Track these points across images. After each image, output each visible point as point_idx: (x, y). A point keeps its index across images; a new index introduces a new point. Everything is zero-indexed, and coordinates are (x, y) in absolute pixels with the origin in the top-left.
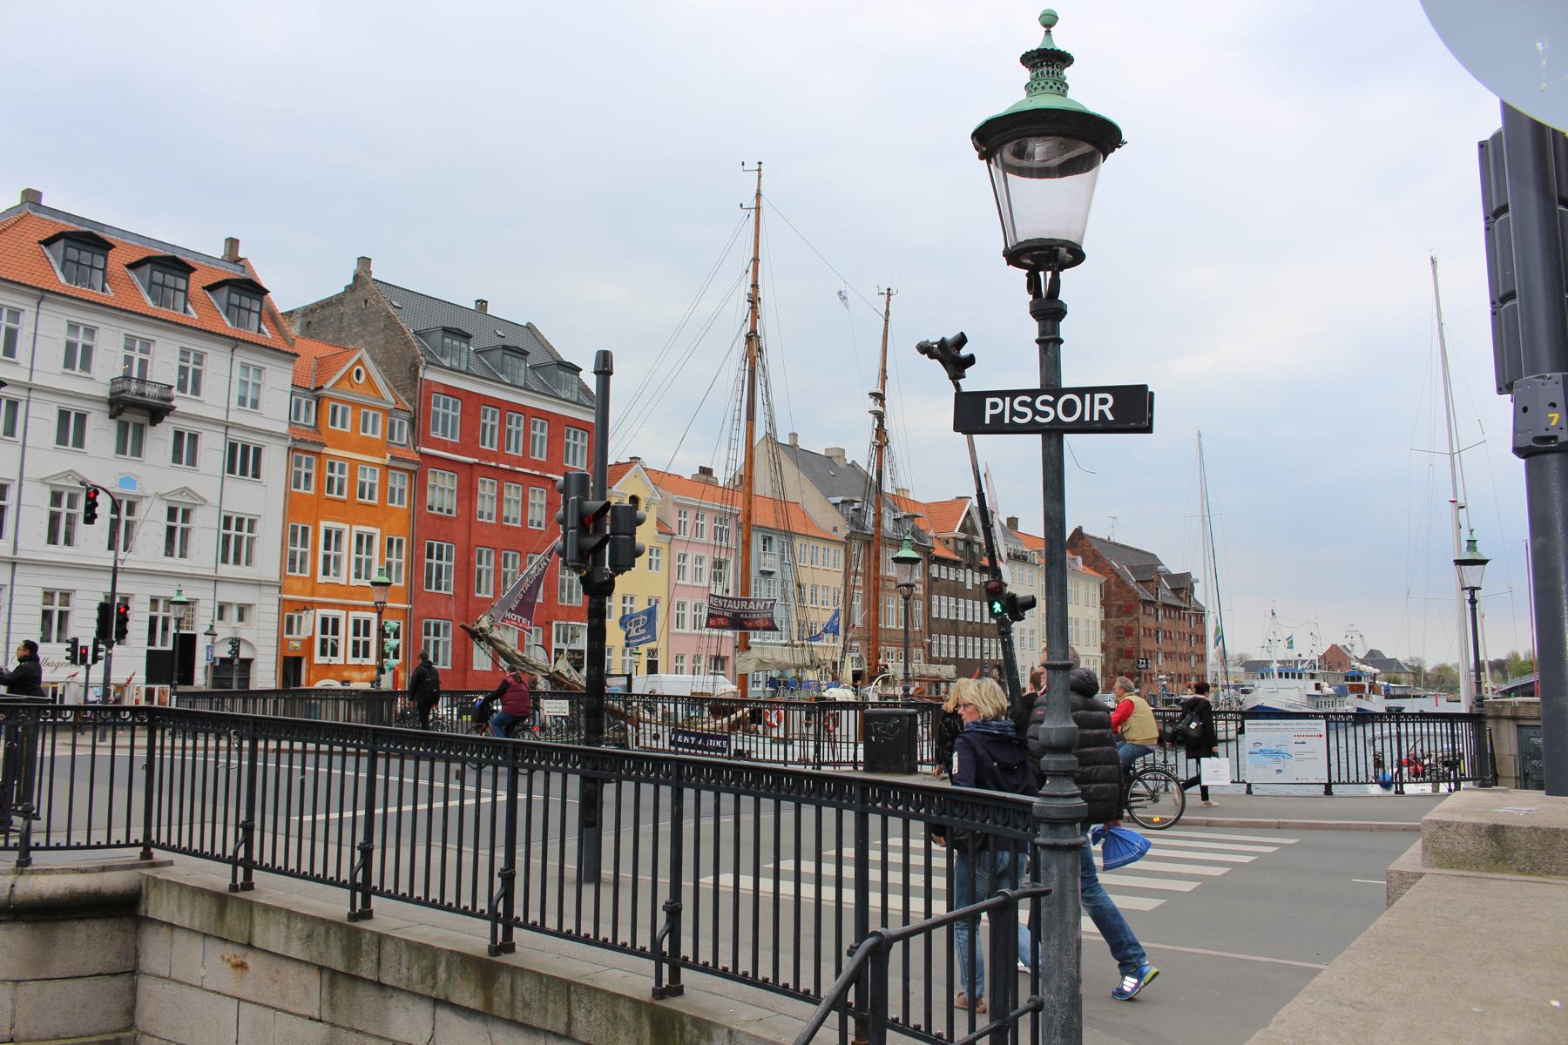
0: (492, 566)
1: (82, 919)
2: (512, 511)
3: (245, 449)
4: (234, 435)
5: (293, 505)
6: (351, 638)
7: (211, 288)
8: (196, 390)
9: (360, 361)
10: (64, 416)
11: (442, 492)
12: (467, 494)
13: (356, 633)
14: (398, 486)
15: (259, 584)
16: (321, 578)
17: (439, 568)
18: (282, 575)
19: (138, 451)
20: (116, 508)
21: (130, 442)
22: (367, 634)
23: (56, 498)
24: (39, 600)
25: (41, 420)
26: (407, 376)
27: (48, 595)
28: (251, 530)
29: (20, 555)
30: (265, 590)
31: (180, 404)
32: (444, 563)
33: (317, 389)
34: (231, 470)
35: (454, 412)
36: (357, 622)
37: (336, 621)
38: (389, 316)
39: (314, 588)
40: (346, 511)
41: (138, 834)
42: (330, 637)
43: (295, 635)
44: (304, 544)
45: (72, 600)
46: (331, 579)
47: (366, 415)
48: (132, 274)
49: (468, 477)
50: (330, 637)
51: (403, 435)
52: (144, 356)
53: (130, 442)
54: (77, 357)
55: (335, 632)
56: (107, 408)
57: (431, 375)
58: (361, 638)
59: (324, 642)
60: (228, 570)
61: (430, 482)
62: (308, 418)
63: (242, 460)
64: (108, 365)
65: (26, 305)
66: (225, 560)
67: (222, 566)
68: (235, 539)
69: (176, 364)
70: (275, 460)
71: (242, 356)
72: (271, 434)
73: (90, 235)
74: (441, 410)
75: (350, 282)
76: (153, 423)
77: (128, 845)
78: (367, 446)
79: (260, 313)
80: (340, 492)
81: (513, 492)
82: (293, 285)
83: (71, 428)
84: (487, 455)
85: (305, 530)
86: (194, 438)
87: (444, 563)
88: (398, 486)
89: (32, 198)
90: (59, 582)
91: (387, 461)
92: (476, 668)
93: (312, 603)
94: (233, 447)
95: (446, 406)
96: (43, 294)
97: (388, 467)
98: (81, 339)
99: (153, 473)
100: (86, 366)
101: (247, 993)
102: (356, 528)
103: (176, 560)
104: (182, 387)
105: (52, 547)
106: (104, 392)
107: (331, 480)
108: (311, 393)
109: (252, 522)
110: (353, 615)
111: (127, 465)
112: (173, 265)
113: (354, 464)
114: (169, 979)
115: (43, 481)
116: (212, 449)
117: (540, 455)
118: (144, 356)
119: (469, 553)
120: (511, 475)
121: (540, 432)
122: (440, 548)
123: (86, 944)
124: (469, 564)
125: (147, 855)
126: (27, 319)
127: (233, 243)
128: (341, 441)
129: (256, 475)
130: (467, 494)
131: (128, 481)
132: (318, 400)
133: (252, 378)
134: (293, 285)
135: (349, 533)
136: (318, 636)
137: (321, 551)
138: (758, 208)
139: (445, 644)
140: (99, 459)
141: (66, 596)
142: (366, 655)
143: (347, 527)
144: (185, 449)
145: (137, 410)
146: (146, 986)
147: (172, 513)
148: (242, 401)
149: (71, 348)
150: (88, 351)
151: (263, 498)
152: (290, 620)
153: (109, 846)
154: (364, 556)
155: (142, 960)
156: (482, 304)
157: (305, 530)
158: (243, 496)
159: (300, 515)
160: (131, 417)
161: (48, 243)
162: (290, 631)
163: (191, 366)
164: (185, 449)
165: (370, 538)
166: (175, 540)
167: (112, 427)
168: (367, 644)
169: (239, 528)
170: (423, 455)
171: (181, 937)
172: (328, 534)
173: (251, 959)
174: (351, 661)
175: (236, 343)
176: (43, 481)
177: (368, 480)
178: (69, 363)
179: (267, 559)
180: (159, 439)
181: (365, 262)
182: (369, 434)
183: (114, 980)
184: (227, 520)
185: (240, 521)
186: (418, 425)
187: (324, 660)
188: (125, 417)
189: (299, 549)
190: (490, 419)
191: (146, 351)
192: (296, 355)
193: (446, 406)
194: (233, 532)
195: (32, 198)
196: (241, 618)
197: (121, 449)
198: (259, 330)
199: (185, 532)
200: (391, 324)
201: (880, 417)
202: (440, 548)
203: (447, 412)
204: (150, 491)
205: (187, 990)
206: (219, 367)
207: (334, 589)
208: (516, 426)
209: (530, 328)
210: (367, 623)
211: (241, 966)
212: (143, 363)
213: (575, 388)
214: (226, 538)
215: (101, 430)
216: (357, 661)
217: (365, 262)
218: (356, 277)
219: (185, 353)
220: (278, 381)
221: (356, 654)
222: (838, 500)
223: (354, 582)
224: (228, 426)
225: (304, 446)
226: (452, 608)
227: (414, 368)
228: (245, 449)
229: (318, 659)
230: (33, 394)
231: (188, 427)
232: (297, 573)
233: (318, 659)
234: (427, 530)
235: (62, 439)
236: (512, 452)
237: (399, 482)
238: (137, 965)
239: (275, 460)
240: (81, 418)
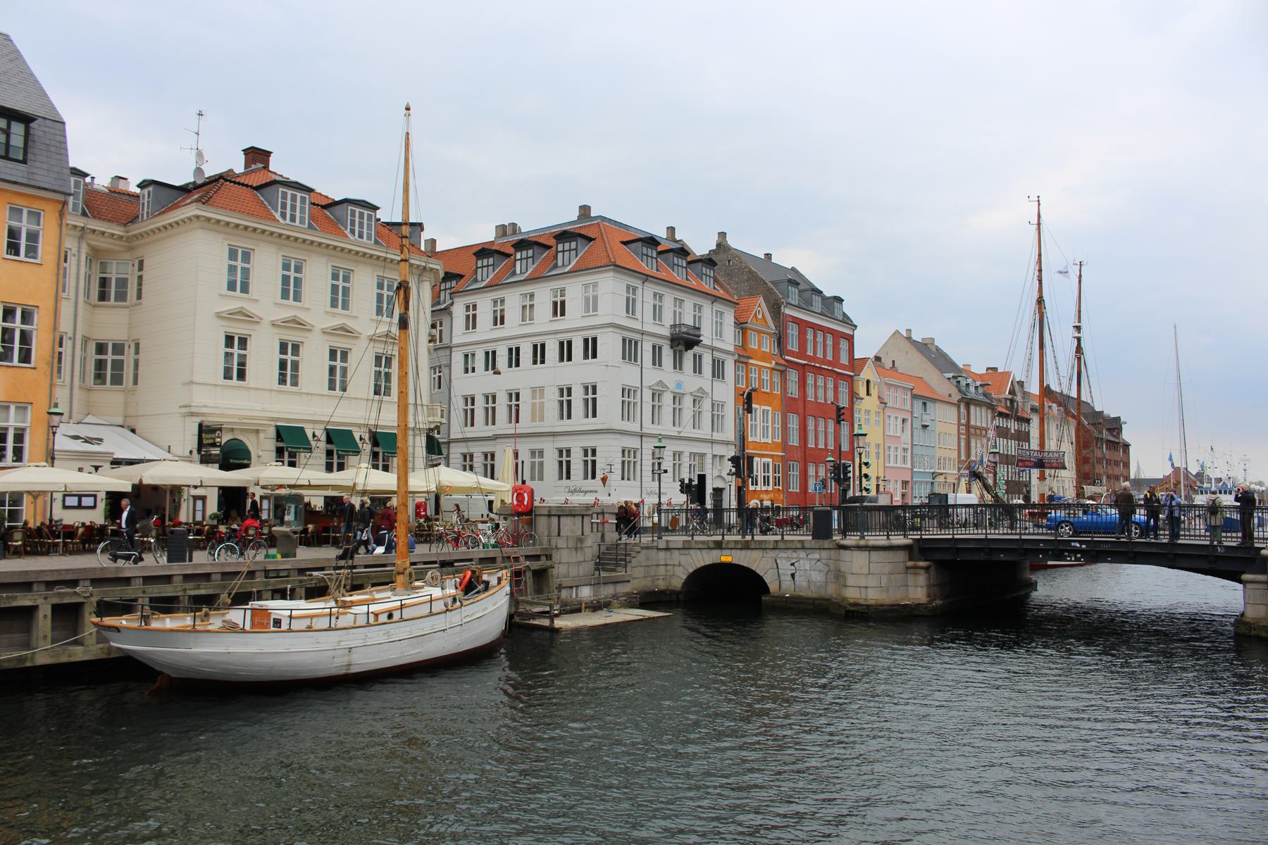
10: (654, 347)
12: (803, 384)
21: (678, 364)
26: (775, 309)
29: (644, 431)
53: (678, 364)
54: (657, 313)
57: (788, 311)
72: (728, 352)
111: (678, 376)
115: (650, 387)
117: (830, 357)
126: (639, 292)
130: (803, 384)
138: (1039, 224)
156: (768, 256)
167: (671, 352)
176: (650, 387)
180: (688, 357)
201: (1079, 339)
203: (793, 331)
204: (687, 391)
209: (793, 269)
218: (718, 245)
222: (950, 375)
224: (713, 349)
240: (660, 348)
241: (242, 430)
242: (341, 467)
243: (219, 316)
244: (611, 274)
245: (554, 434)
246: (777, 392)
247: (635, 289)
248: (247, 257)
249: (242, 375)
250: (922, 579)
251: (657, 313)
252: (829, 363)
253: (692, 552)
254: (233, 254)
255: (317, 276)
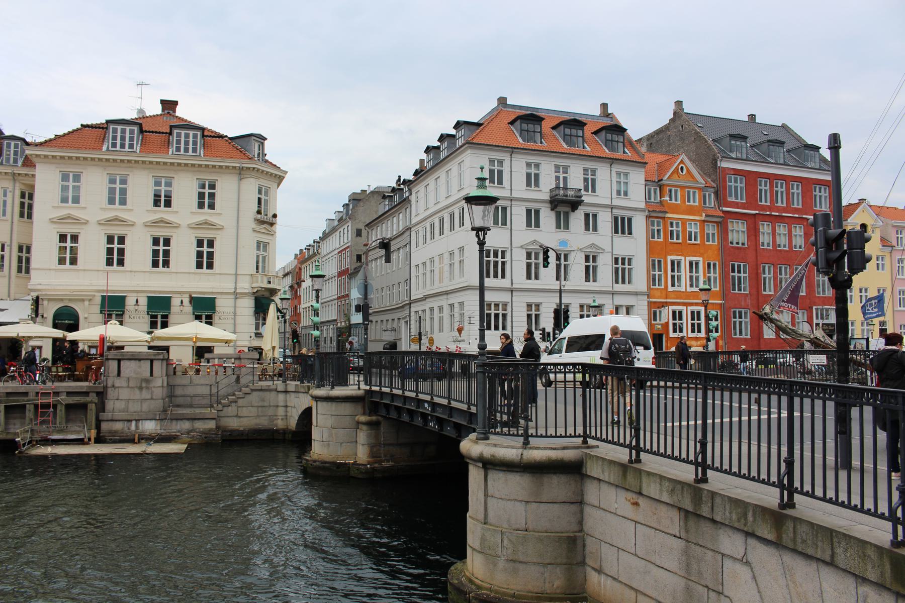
0: (772, 275)
1: (555, 473)
2: (782, 241)
3: (623, 219)
4: (616, 212)
5: (652, 248)
6: (690, 322)
7: (596, 133)
8: (594, 190)
9: (682, 162)
10: (529, 212)
11: (738, 233)
12: (753, 233)
13: (693, 319)
14: (711, 232)
15: (636, 294)
16: (670, 289)
17: (739, 278)
18: (649, 288)
19: (567, 227)
20: (558, 258)
21: (562, 223)
22: (699, 319)
23: (529, 256)
24: (525, 309)
25: (518, 215)
26: (710, 167)
27: (529, 306)
28: (629, 264)
29: (514, 286)
30: (639, 297)
31: (586, 199)
32: (742, 275)
33: (659, 181)
34: (616, 232)
35: (741, 184)
36: (692, 313)
37: (680, 313)
38: (697, 133)
39: (667, 295)
40: (682, 249)
41: (580, 431)
42: (677, 322)
43: (658, 322)
44: (660, 270)
45: (541, 308)
46: (676, 288)
47: (689, 192)
48: (554, 132)
49: (753, 223)
50: (677, 322)
51: (712, 201)
52: (565, 175)
53: (562, 223)
54: (532, 180)
55: (681, 319)
56: (549, 205)
57: (725, 164)
58: (696, 322)
59: (674, 325)
60: (619, 287)
61: (730, 228)
62: (655, 198)
63: (622, 226)
64: (547, 182)
65: (504, 156)
66: (617, 282)
67: (615, 285)
68: (622, 269)
69: (582, 177)
70: (639, 224)
71: (616, 168)
72: (636, 209)
73: (532, 115)
74: (733, 184)
75: (672, 116)
76: (573, 211)
77: (575, 436)
78: (691, 211)
79: (623, 143)
80: (678, 238)
81: (782, 229)
82: (639, 125)
83: (533, 218)
84: (763, 208)
85: (659, 262)
86: (595, 216)
87: (742, 275)
88: (711, 232)
89: (502, 101)
90: (534, 299)
91: (703, 218)
92: (765, 336)
93: (666, 303)
94: (616, 219)
95: (736, 181)
96: (513, 150)
97: (704, 221)
98: (533, 171)
99: (576, 237)
100: (537, 184)
101: (640, 518)
102: (688, 259)
103: (591, 283)
104: (586, 189)
105: (529, 281)
106: (547, 197)
107: (672, 232)
108: (656, 184)
109: (630, 260)
110: (690, 308)
111: (562, 235)
112: (572, 124)
113: (684, 222)
114: (599, 507)
115: (522, 247)
116: (605, 221)
117: (797, 204)
118: (565, 175)
119: (757, 267)
120: (780, 219)
121: (796, 190)
122: (739, 266)
123: (557, 486)
124: (757, 275)
125: (585, 442)
126: (507, 164)
127: (604, 106)
128: (676, 209)
129: (630, 233)
130: (753, 233)
131: (563, 243)
132: (661, 187)
133: (622, 180)
134: (639, 125)
135: (685, 261)
136: (671, 322)
137: (670, 273)
139: (746, 323)
140: (548, 234)
141: (538, 306)
142: (699, 331)
143: (683, 258)
144: (591, 222)
145: (564, 204)
146: (588, 510)
147: (587, 258)
148: (619, 193)
149: (528, 176)
150: (537, 176)
151: (635, 246)
152: (655, 313)
153: (566, 436)
154: (694, 274)
155: (585, 497)
156: (752, 117)
157: (659, 262)
158: (625, 246)
159: (656, 253)
160: (562, 209)
161: (512, 123)
162: (655, 319)
163: (590, 177)
164: (591, 222)
165: (697, 264)
166: (590, 273)
167: (553, 215)
168: (699, 325)
169: (623, 264)
170: (724, 212)
171: (604, 487)
172: (673, 263)
173: (641, 501)
174: (691, 335)
175: (612, 161)
176: (522, 247)
177: (693, 230)
178: (529, 184)
179: (640, 281)
180: (577, 219)
181: (679, 103)
182: (691, 203)
183: (572, 506)
184: (616, 260)
185: (623, 259)
186: (720, 195)
187: (675, 335)
188: (559, 209)
189: (657, 273)
190: (764, 186)
191: (565, 172)
192: (646, 163)
193: (736, 181)
194: (620, 266)
195: (502, 101)
196: (628, 313)
197: (558, 226)
198: (624, 152)
199: (595, 268)
200: (698, 137)
202: (739, 266)
203: (737, 185)
204: (575, 247)
205: (608, 514)
206: (604, 175)
207: (678, 294)
208: (780, 188)
209: (784, 127)
210: (699, 313)
211: (636, 504)
212: (565, 179)
213: (817, 160)
214: (617, 270)
215: (547, 217)
216: (694, 335)
217: (679, 103)
218: (675, 113)
219: (586, 170)
220: (637, 179)
221: (693, 331)
223: (689, 289)
224: (612, 208)
225: (656, 214)
226: (749, 302)
227: (715, 161)
228: (623, 219)
229: (672, 335)
230: (513, 203)
231: (591, 210)
232: (657, 287)
233: (672, 335)
234: (730, 256)
235: (529, 224)
236: (779, 204)
237: (711, 229)
238: (583, 499)
239: (639, 224)
240: (537, 212)
241: (70, 300)
242: (165, 325)
243: (52, 221)
244: (469, 151)
245: (447, 293)
246: (714, 243)
247: (501, 162)
248: (77, 178)
249: (74, 261)
250: (363, 436)
251: (532, 180)
252: (796, 211)
253: (301, 395)
254: (65, 177)
255: (141, 187)
